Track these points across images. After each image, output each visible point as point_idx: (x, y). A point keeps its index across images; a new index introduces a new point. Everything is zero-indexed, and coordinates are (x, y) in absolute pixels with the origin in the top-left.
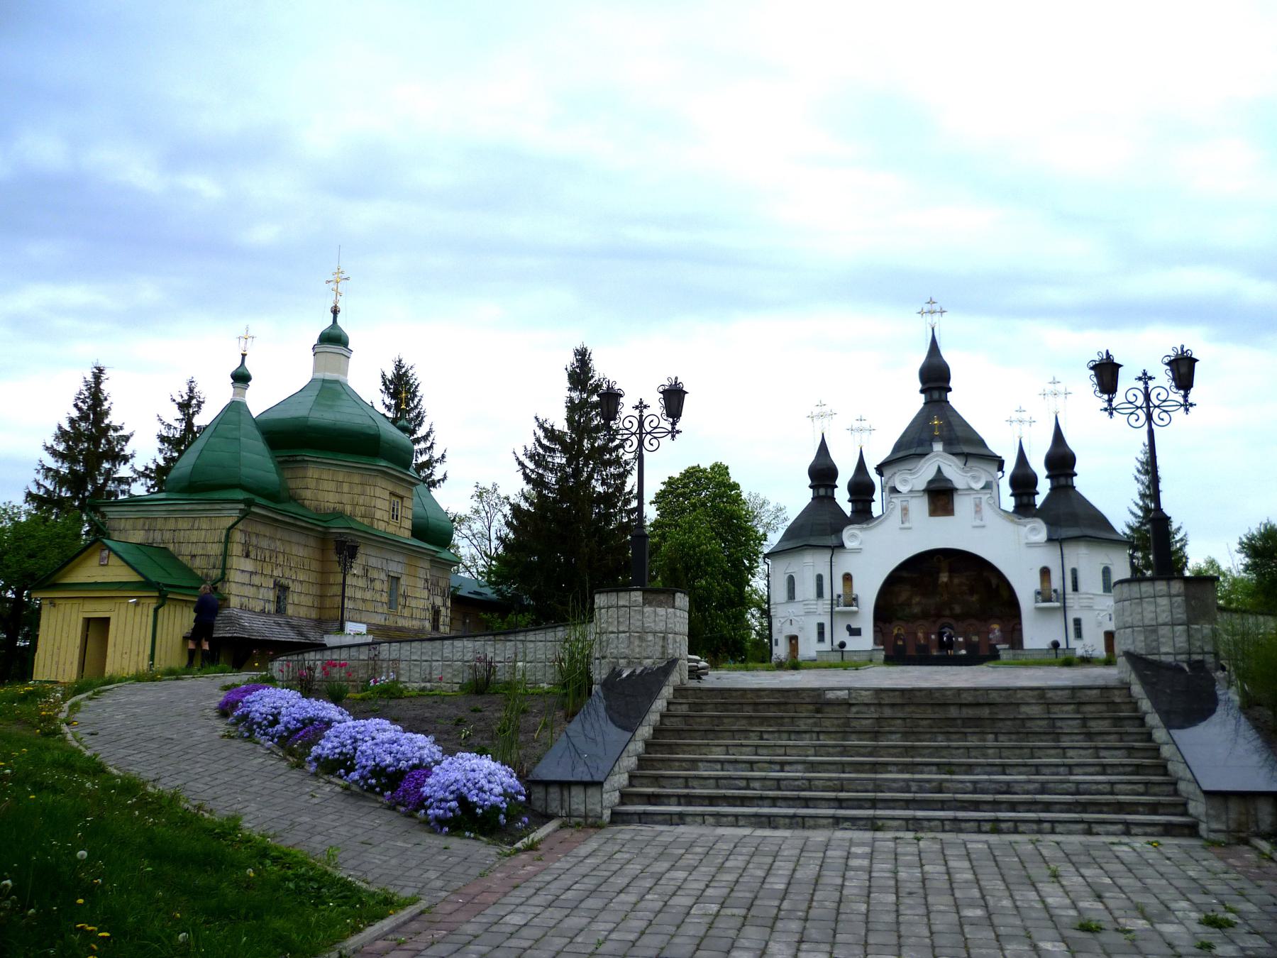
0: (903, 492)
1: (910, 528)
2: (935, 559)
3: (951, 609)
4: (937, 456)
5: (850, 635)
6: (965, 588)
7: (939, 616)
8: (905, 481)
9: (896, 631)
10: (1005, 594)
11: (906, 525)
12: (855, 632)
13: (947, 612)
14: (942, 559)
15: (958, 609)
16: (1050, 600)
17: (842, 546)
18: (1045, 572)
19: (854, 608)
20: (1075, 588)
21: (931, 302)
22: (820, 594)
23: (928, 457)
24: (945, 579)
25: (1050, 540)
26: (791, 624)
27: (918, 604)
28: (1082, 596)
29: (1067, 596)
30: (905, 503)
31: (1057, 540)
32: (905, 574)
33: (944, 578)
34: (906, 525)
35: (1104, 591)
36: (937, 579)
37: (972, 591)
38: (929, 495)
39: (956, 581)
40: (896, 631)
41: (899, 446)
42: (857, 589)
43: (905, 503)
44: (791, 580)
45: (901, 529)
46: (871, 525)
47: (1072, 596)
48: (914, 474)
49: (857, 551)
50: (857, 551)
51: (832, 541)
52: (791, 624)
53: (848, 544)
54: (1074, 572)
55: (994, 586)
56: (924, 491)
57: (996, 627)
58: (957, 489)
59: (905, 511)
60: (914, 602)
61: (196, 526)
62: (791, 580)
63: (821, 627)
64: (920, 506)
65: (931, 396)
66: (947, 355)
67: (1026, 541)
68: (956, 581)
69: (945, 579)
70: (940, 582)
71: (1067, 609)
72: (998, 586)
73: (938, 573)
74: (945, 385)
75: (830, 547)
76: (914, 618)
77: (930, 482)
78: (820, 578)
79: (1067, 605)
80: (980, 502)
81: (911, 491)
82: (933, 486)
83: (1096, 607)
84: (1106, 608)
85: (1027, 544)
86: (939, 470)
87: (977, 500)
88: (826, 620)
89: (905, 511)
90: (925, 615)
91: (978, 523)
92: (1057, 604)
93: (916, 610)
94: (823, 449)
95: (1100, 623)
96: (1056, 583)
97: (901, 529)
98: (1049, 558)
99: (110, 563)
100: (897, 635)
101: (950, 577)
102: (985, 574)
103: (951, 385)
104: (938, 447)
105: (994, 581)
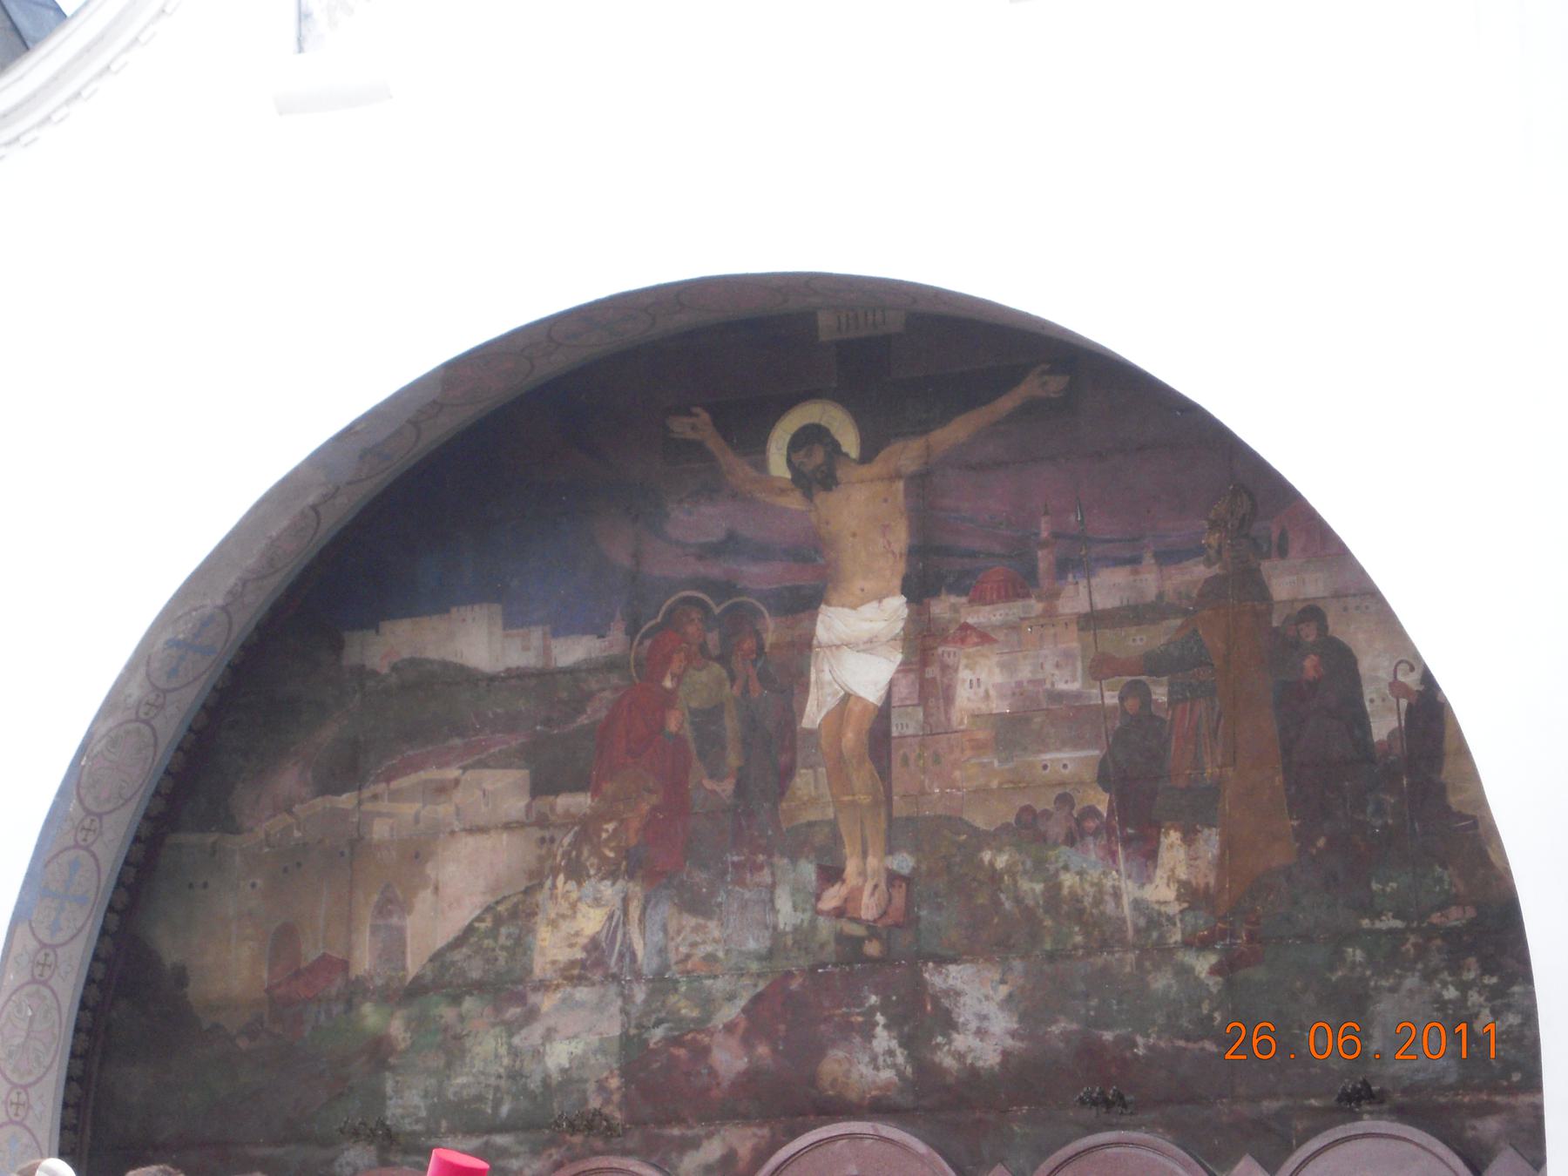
14: (849, 441)
70: (814, 714)
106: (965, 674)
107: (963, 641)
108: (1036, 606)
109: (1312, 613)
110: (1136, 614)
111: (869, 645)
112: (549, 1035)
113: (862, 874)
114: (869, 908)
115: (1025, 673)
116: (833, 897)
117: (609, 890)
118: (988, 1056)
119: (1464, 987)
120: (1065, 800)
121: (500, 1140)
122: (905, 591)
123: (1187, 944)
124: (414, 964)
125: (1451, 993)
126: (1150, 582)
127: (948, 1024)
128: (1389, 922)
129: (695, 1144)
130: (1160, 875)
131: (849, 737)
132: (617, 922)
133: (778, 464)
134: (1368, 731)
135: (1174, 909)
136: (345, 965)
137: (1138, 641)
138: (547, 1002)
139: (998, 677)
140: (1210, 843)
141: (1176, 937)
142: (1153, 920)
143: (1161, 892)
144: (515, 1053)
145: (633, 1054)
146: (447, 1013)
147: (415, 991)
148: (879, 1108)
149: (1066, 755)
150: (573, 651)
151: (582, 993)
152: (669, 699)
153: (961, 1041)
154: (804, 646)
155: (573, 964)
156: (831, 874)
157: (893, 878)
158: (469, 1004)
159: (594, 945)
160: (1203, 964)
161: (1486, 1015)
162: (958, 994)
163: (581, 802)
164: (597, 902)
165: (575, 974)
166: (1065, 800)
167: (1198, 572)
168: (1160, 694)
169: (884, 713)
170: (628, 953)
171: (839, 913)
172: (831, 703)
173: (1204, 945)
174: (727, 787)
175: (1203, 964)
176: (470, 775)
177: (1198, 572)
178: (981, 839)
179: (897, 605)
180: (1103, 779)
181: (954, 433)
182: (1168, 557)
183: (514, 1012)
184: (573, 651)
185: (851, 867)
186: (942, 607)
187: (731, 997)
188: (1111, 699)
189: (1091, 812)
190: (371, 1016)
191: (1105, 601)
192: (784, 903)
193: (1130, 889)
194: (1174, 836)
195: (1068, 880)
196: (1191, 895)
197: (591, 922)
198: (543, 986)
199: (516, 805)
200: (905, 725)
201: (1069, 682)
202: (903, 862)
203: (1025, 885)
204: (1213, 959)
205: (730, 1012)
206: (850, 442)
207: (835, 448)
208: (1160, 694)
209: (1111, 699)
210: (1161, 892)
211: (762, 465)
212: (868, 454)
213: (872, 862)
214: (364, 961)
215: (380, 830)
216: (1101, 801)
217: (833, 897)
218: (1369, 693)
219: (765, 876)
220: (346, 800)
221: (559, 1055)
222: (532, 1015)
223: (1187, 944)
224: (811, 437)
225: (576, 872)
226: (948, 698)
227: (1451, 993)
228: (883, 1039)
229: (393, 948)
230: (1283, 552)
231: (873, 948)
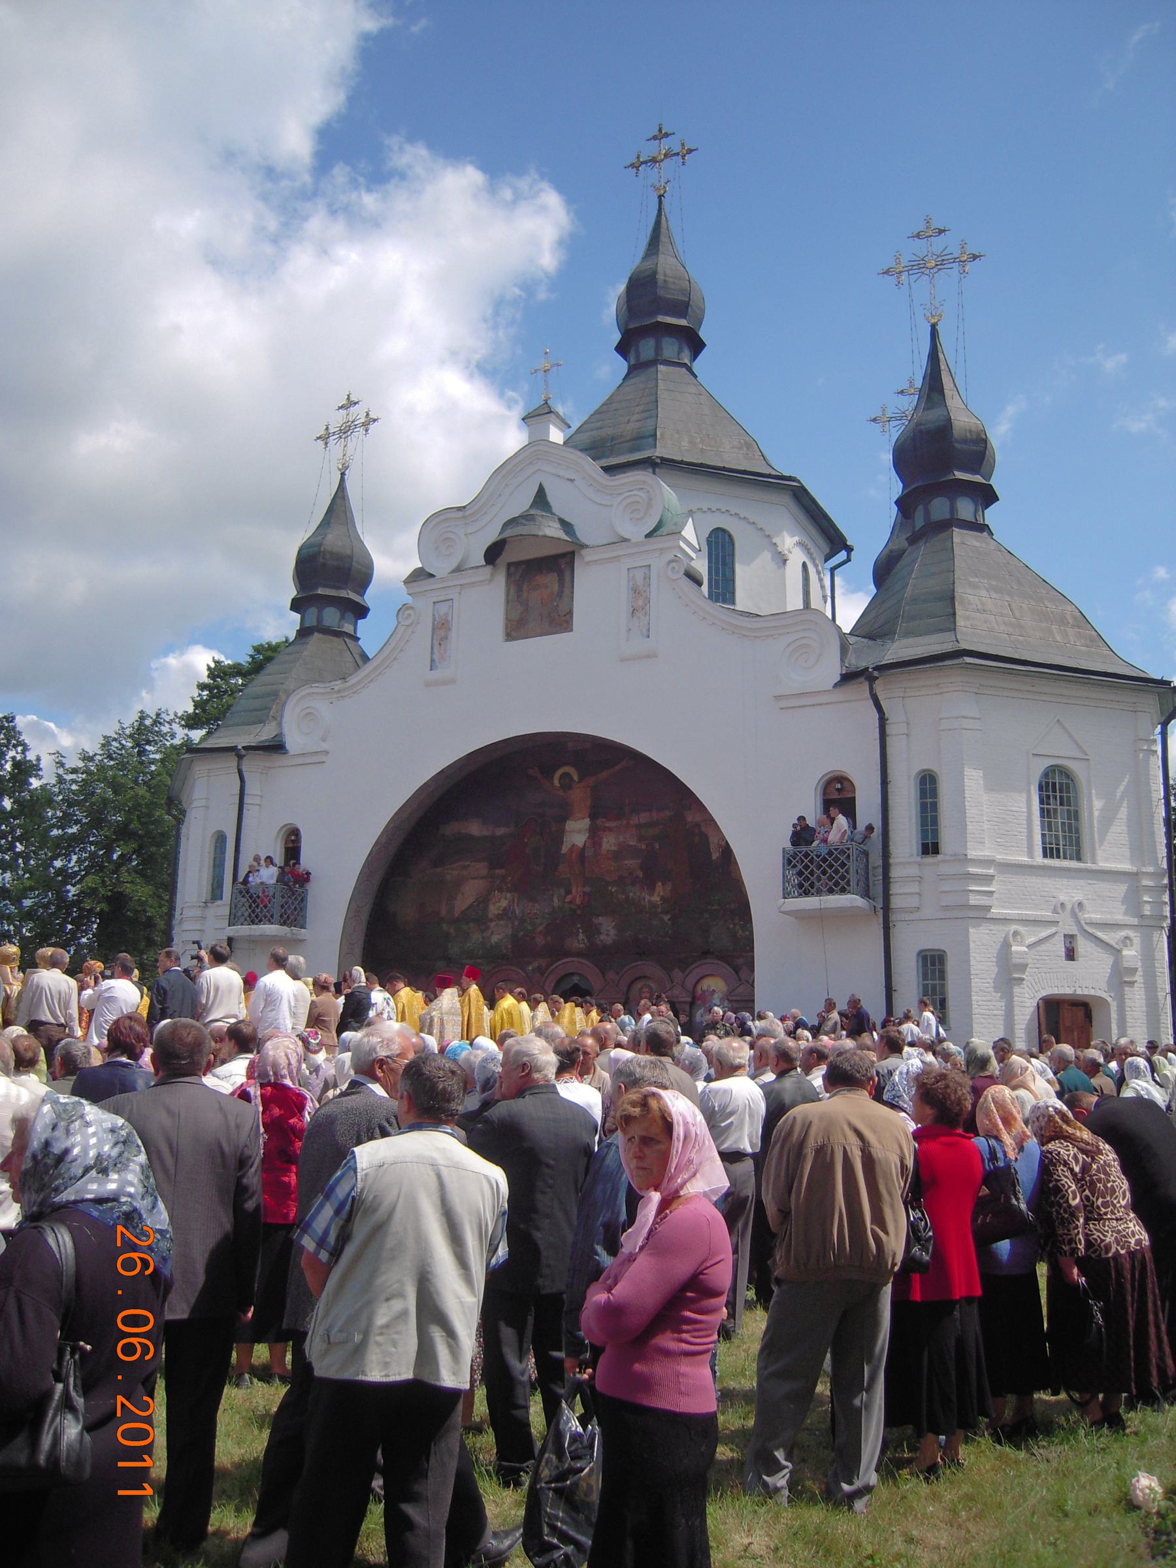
1: (452, 681)
3: (592, 931)
6: (632, 863)
7: (557, 952)
11: (440, 673)
13: (579, 941)
14: (576, 778)
15: (608, 931)
17: (276, 747)
20: (930, 848)
21: (661, 135)
25: (848, 678)
27: (505, 914)
28: (945, 869)
29: (895, 873)
33: (576, 833)
35: (1045, 856)
37: (650, 876)
38: (509, 575)
39: (609, 842)
43: (443, 609)
45: (428, 684)
47: (914, 871)
49: (315, 759)
50: (315, 759)
53: (294, 741)
54: (928, 784)
58: (587, 546)
60: (494, 910)
68: (609, 842)
70: (564, 850)
73: (562, 819)
75: (233, 749)
80: (647, 578)
81: (458, 570)
83: (995, 911)
84: (1056, 917)
85: (778, 698)
87: (639, 575)
93: (498, 935)
95: (1023, 967)
97: (428, 684)
106: (605, 840)
107: (604, 831)
108: (624, 822)
109: (698, 825)
111: (579, 832)
112: (492, 933)
113: (577, 892)
114: (578, 901)
115: (621, 839)
116: (568, 899)
117: (508, 895)
118: (609, 941)
119: (735, 925)
120: (631, 874)
121: (479, 961)
123: (662, 912)
124: (456, 915)
125: (731, 926)
127: (600, 933)
128: (715, 907)
129: (529, 963)
130: (655, 895)
131: (574, 855)
133: (556, 782)
134: (711, 856)
135: (659, 903)
138: (492, 925)
139: (614, 841)
140: (669, 887)
141: (660, 910)
142: (653, 905)
143: (656, 898)
144: (483, 938)
146: (465, 927)
148: (579, 954)
149: (632, 862)
150: (501, 831)
151: (502, 922)
153: (602, 937)
154: (562, 832)
155: (498, 915)
156: (568, 892)
157: (584, 893)
158: (471, 925)
159: (505, 909)
160: (666, 918)
161: (740, 932)
162: (601, 924)
163: (503, 871)
164: (506, 899)
165: (499, 917)
166: (631, 874)
167: (668, 813)
168: (657, 846)
169: (583, 849)
170: (514, 912)
171: (570, 902)
172: (569, 846)
173: (667, 912)
175: (666, 918)
176: (473, 864)
177: (668, 813)
179: (587, 821)
181: (604, 775)
183: (483, 927)
184: (501, 831)
185: (574, 891)
186: (599, 822)
187: (541, 924)
188: (644, 847)
189: (638, 877)
191: (643, 821)
192: (556, 900)
193: (647, 898)
194: (660, 884)
195: (631, 895)
196: (662, 898)
197: (504, 903)
198: (491, 920)
199: (484, 872)
200: (589, 853)
202: (587, 889)
203: (620, 896)
204: (669, 917)
205: (541, 928)
206: (576, 778)
207: (571, 779)
208: (657, 846)
209: (644, 847)
210: (656, 898)
211: (552, 783)
212: (579, 782)
213: (579, 889)
214: (443, 912)
215: (448, 877)
217: (568, 899)
218: (712, 846)
219: (551, 892)
220: (439, 870)
221: (495, 939)
222: (488, 928)
223: (662, 912)
225: (500, 890)
226: (600, 845)
227: (731, 926)
228: (581, 936)
230: (690, 809)
231: (579, 912)
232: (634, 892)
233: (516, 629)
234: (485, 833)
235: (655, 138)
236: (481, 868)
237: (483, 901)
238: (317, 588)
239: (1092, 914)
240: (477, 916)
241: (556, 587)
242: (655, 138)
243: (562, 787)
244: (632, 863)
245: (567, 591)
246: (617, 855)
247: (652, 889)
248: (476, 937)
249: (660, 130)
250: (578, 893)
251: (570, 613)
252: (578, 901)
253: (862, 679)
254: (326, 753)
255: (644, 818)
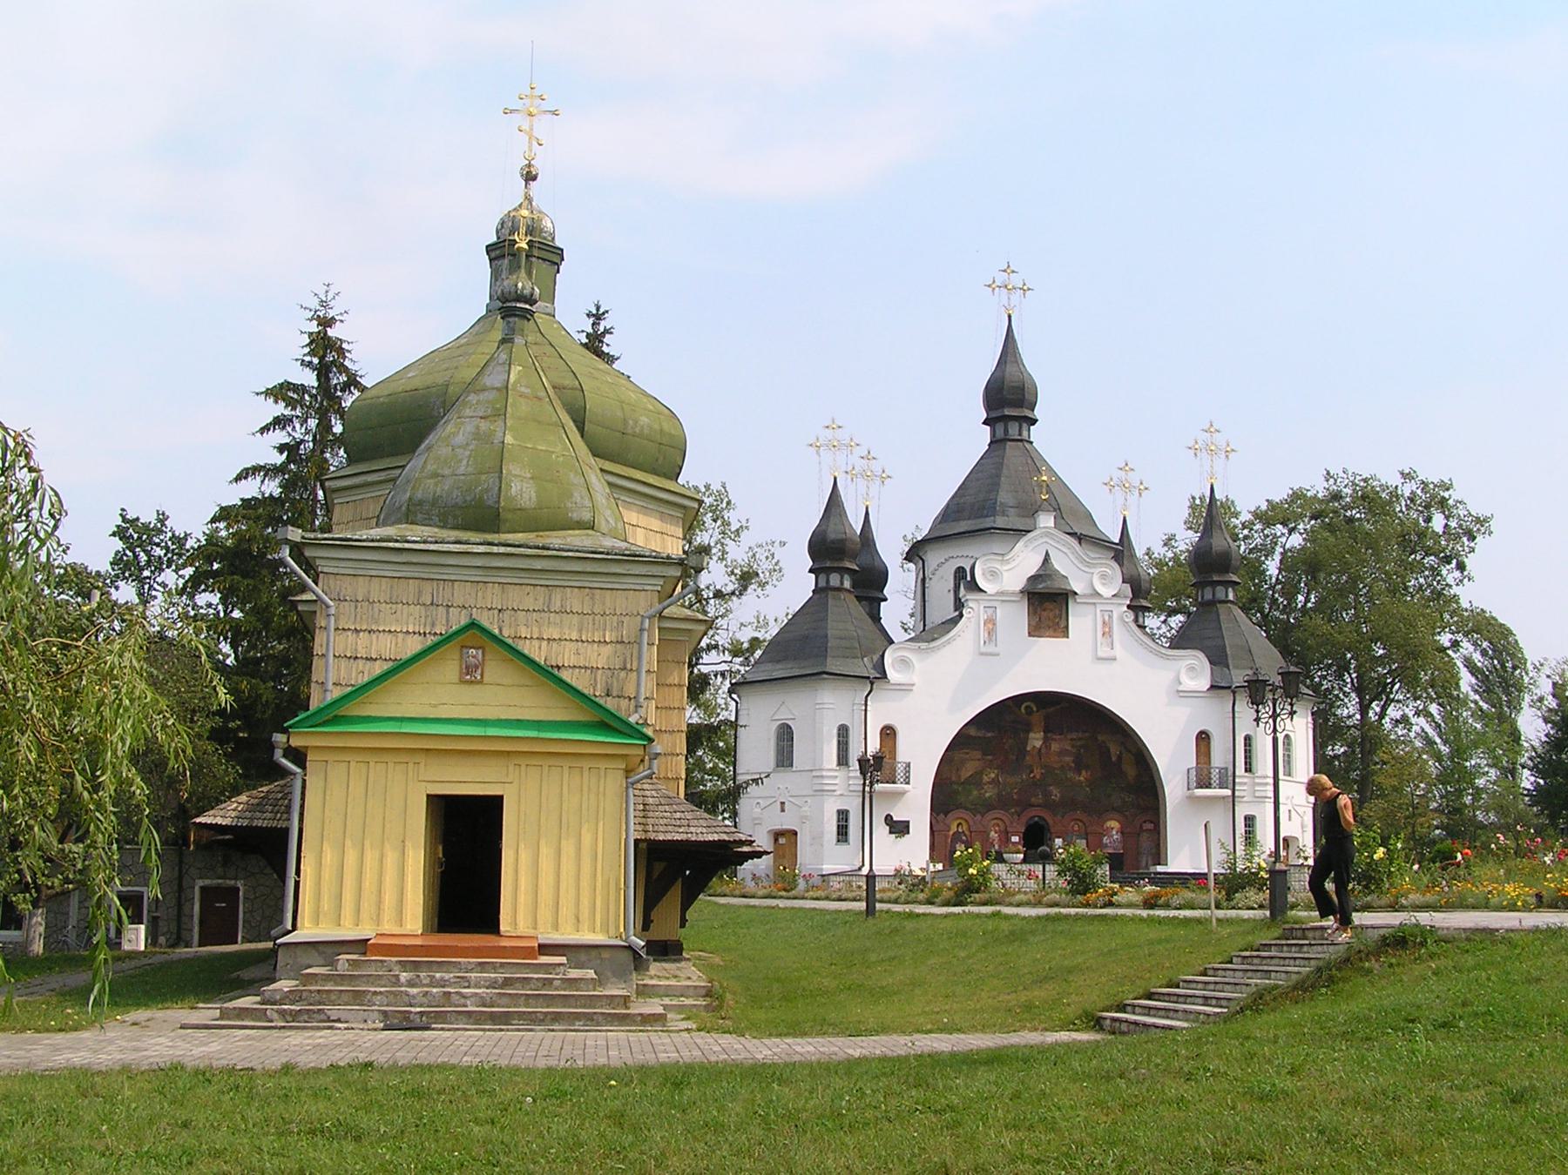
0: (989, 592)
1: (998, 655)
2: (1023, 706)
3: (1047, 794)
4: (1047, 534)
5: (891, 832)
8: (993, 575)
9: (954, 828)
10: (1131, 771)
11: (990, 648)
12: (899, 828)
14: (1035, 709)
15: (1056, 793)
16: (1208, 786)
18: (1203, 738)
19: (899, 786)
20: (1248, 769)
22: (843, 760)
23: (1030, 535)
24: (1038, 744)
25: (1212, 687)
26: (783, 810)
27: (994, 782)
28: (1257, 781)
30: (990, 611)
31: (1230, 687)
32: (973, 732)
33: (1036, 740)
34: (990, 648)
36: (1025, 744)
37: (1079, 766)
40: (954, 828)
41: (952, 512)
42: (904, 753)
44: (785, 735)
45: (982, 654)
46: (933, 644)
47: (1245, 780)
48: (1008, 562)
49: (905, 688)
50: (905, 688)
51: (865, 667)
52: (783, 810)
54: (1248, 739)
55: (1114, 759)
56: (1022, 592)
57: (1114, 824)
58: (1076, 593)
59: (991, 622)
60: (986, 779)
61: (556, 606)
62: (785, 735)
63: (843, 816)
64: (1017, 617)
65: (1006, 431)
66: (1035, 363)
67: (1180, 688)
68: (1055, 747)
69: (1038, 744)
70: (1028, 749)
71: (1236, 799)
72: (1120, 758)
73: (1028, 732)
74: (1027, 413)
75: (868, 678)
76: (988, 807)
77: (1033, 579)
78: (843, 732)
79: (1237, 793)
82: (1040, 587)
86: (1047, 559)
88: (853, 806)
89: (991, 622)
90: (1002, 803)
91: (1104, 651)
92: (1228, 792)
94: (834, 504)
96: (1219, 758)
97: (982, 654)
98: (1212, 715)
99: (486, 679)
100: (957, 833)
101: (1046, 740)
102: (1100, 738)
103: (1037, 413)
104: (1046, 521)
105: (1114, 750)
109: (1104, 742)
110: (1080, 739)
114: (1038, 777)
122: (1044, 732)
126: (1080, 735)
132: (997, 775)
136: (950, 779)
137: (1079, 743)
143: (1082, 778)
145: (999, 795)
147: (963, 783)
150: (989, 735)
152: (1004, 744)
156: (1032, 772)
163: (990, 757)
167: (1087, 734)
169: (1040, 750)
174: (1014, 758)
178: (1055, 769)
180: (1073, 762)
181: (1052, 709)
182: (1084, 732)
184: (989, 735)
186: (1049, 735)
190: (955, 787)
197: (993, 775)
200: (1043, 751)
201: (1069, 748)
206: (1035, 709)
214: (954, 779)
216: (1073, 765)
221: (987, 795)
224: (1027, 707)
229: (960, 776)
232: (1070, 775)
233: (1036, 630)
234: (979, 734)
235: (1005, 271)
236: (978, 755)
237: (979, 774)
238: (841, 560)
239: (1295, 802)
240: (975, 780)
241: (1057, 612)
242: (1005, 271)
243: (1027, 713)
244: (1068, 759)
245: (1064, 612)
246: (1062, 753)
247: (1080, 775)
248: (975, 793)
249: (1009, 266)
250: (1037, 773)
251: (1067, 627)
252: (1038, 777)
253: (1229, 691)
254: (913, 685)
255: (1074, 735)
